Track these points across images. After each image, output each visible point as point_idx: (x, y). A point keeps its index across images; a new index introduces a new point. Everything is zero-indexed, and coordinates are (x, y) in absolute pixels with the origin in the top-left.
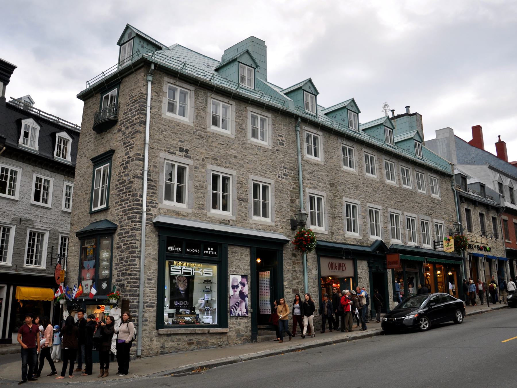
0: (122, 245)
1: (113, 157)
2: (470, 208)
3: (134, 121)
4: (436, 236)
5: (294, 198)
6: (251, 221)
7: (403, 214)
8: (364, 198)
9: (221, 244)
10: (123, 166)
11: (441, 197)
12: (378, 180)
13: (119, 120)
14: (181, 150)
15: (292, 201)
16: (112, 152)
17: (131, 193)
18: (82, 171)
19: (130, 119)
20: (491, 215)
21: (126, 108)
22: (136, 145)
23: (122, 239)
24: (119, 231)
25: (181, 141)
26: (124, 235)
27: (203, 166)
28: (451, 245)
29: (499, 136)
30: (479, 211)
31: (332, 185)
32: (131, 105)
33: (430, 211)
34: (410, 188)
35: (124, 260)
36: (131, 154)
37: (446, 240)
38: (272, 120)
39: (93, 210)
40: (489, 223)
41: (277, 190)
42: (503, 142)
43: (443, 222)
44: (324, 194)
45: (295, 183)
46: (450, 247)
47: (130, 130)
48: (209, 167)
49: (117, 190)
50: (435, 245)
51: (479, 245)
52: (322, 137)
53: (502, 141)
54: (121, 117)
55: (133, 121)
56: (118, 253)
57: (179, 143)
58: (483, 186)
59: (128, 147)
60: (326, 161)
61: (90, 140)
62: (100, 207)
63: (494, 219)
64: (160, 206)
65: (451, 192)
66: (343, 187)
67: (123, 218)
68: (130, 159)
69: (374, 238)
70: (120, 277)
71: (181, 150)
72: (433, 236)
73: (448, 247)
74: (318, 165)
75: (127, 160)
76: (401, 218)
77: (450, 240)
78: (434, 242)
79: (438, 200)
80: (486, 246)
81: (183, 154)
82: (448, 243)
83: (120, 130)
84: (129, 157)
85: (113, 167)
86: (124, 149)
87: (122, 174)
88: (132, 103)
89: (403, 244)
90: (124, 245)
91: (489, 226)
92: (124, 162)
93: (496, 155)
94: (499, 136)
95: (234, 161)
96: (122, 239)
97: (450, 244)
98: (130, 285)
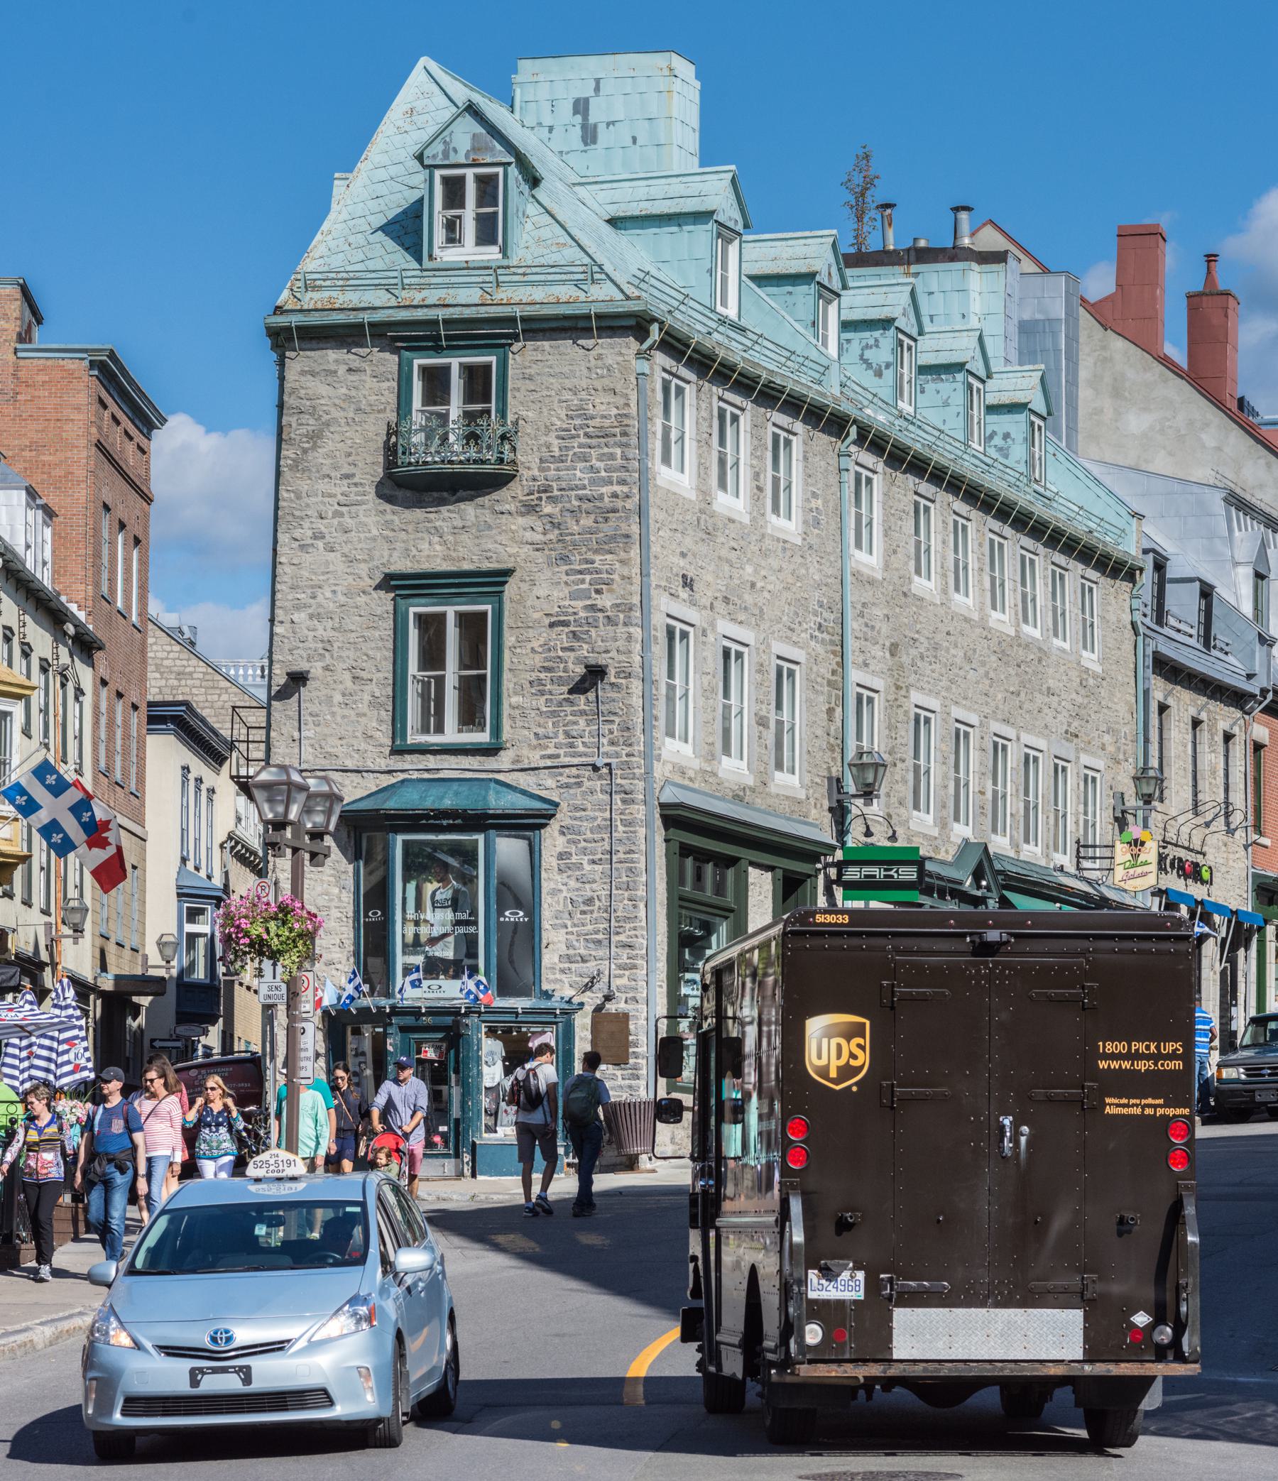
0: (585, 862)
1: (510, 590)
2: (1170, 702)
3: (606, 499)
4: (1082, 817)
5: (833, 705)
6: (773, 789)
7: (1018, 739)
8: (948, 689)
9: (732, 861)
10: (566, 630)
11: (1102, 660)
12: (976, 616)
13: (523, 472)
14: (688, 583)
15: (830, 711)
16: (508, 573)
17: (617, 720)
18: (320, 598)
19: (584, 488)
20: (1223, 725)
21: (556, 442)
22: (623, 578)
23: (583, 844)
24: (563, 817)
25: (683, 555)
26: (589, 835)
27: (713, 625)
28: (1146, 863)
29: (1211, 258)
30: (1193, 711)
31: (894, 649)
32: (583, 440)
33: (1076, 723)
34: (1037, 633)
35: (597, 903)
36: (606, 601)
37: (1129, 843)
38: (805, 443)
39: (414, 738)
40: (1211, 758)
41: (811, 685)
42: (1227, 294)
43: (1100, 764)
44: (877, 683)
45: (834, 653)
46: (1139, 870)
47: (587, 522)
48: (725, 627)
49: (543, 699)
50: (1078, 857)
51: (1182, 854)
52: (881, 477)
53: (1222, 287)
54: (528, 460)
55: (601, 497)
56: (566, 884)
57: (682, 563)
58: (1207, 592)
59: (588, 578)
60: (887, 567)
61: (353, 497)
62: (452, 734)
63: (1228, 737)
64: (665, 755)
65: (1129, 633)
66: (913, 652)
67: (579, 784)
68: (600, 615)
69: (962, 831)
70: (582, 951)
71: (688, 583)
72: (1077, 823)
73: (1131, 871)
74: (871, 582)
75: (582, 614)
76: (1014, 757)
77: (1143, 844)
78: (1078, 842)
79: (1095, 676)
80: (1199, 859)
81: (684, 594)
82: (1135, 857)
83: (530, 509)
84: (592, 608)
85: (507, 620)
86: (565, 578)
87: (560, 653)
88: (587, 435)
89: (1012, 854)
90: (594, 862)
91: (1214, 772)
92: (572, 618)
93: (1185, 365)
94: (1211, 258)
95: (749, 598)
96: (583, 844)
97: (1142, 858)
98: (627, 973)
